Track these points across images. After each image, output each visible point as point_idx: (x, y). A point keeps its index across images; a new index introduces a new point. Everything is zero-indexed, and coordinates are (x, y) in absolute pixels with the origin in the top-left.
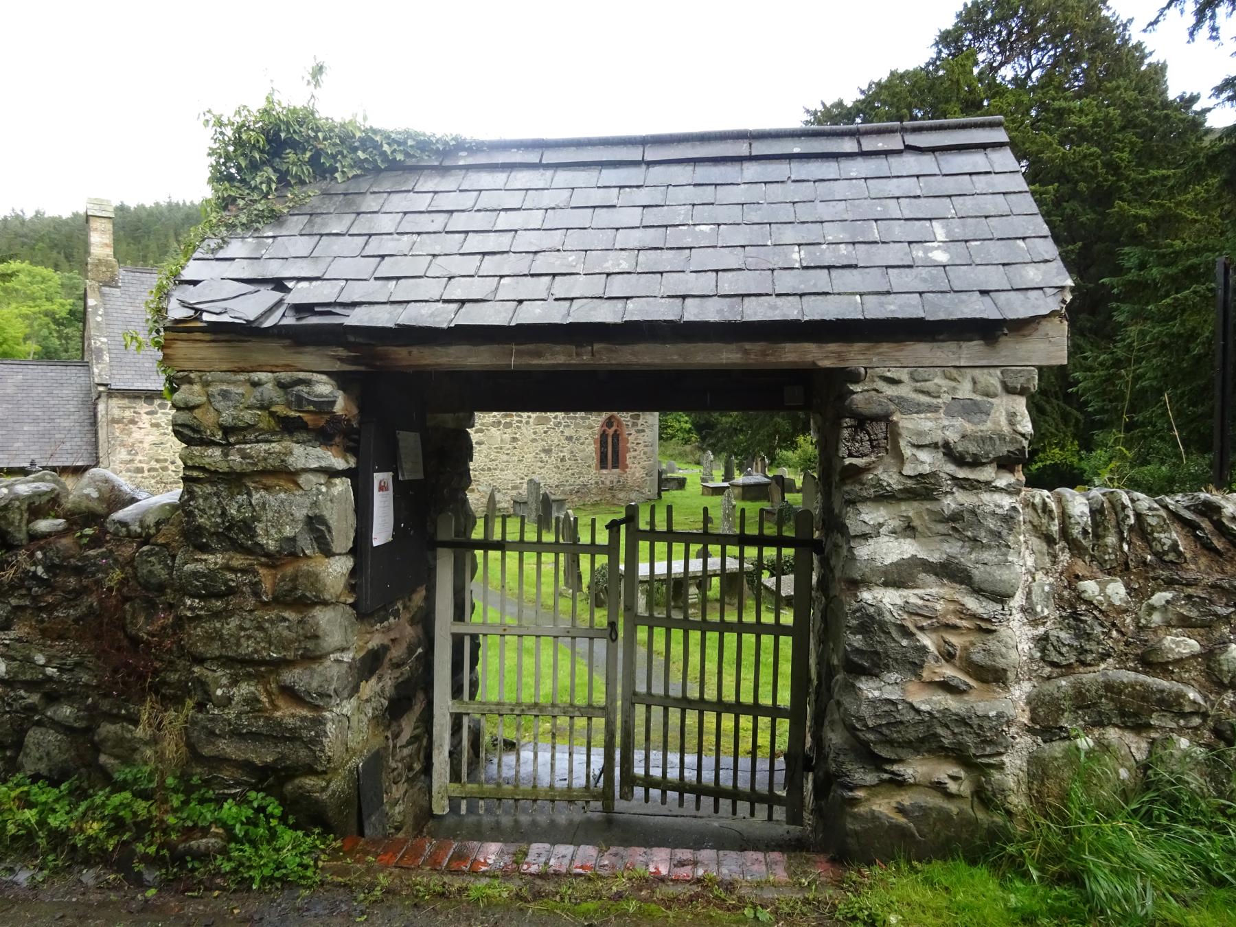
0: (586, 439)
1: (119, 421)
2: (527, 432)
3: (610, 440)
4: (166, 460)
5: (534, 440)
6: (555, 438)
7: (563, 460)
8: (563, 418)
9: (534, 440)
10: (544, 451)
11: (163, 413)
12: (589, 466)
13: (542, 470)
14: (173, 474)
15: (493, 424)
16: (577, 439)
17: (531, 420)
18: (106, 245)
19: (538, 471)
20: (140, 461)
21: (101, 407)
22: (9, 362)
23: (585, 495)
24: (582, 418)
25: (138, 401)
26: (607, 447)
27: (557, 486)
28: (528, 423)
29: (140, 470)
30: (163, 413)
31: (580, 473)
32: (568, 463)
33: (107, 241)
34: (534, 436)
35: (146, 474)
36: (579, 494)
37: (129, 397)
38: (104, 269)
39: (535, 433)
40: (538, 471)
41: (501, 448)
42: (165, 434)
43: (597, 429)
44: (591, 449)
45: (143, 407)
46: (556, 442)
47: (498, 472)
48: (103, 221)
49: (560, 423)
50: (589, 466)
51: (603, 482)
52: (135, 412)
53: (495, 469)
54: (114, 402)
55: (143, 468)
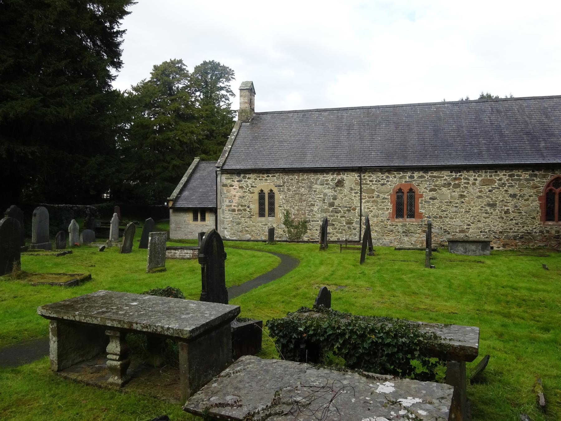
0: (530, 196)
1: (225, 185)
2: (474, 191)
3: (557, 197)
4: (245, 206)
5: (480, 197)
6: (499, 196)
7: (507, 212)
8: (508, 180)
9: (480, 197)
10: (489, 205)
11: (244, 181)
12: (534, 218)
13: (487, 220)
14: (249, 213)
15: (444, 185)
16: (521, 196)
17: (477, 182)
18: (246, 103)
19: (483, 220)
20: (234, 206)
21: (219, 179)
22: (211, 162)
23: (530, 241)
24: (526, 180)
25: (234, 175)
26: (554, 203)
27: (501, 232)
28: (474, 184)
29: (234, 210)
30: (244, 181)
31: (524, 223)
32: (512, 215)
33: (246, 101)
34: (479, 194)
35: (236, 212)
36: (523, 240)
37: (230, 173)
38: (244, 114)
39: (480, 192)
40: (483, 220)
41: (450, 202)
42: (245, 192)
43: (542, 189)
44: (535, 204)
45: (236, 178)
46: (500, 198)
47: (447, 220)
48: (245, 91)
49: (504, 184)
50: (534, 218)
51: (548, 232)
52: (232, 181)
53: (446, 217)
54: (224, 177)
55: (235, 209)
